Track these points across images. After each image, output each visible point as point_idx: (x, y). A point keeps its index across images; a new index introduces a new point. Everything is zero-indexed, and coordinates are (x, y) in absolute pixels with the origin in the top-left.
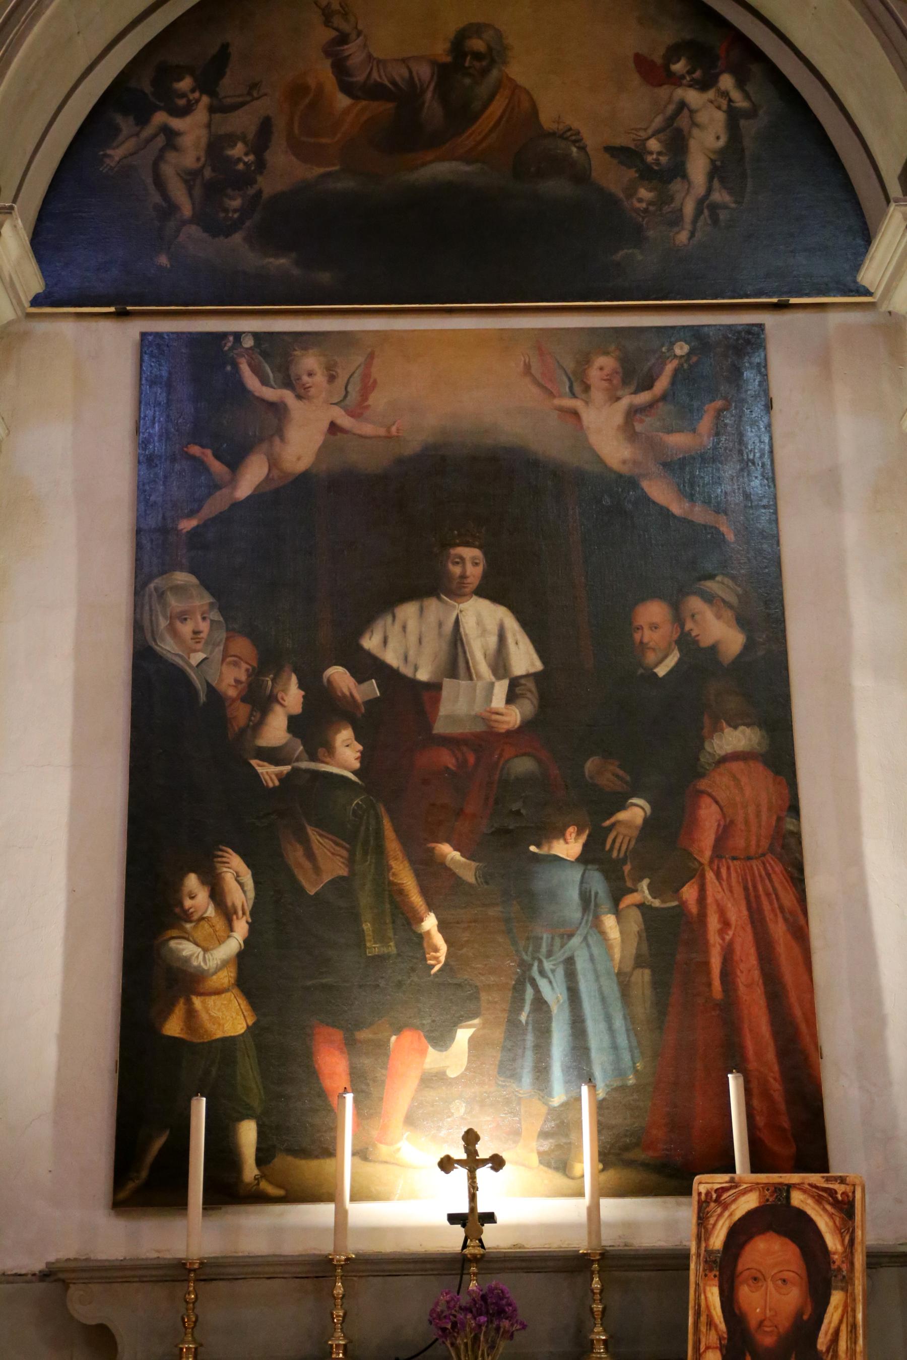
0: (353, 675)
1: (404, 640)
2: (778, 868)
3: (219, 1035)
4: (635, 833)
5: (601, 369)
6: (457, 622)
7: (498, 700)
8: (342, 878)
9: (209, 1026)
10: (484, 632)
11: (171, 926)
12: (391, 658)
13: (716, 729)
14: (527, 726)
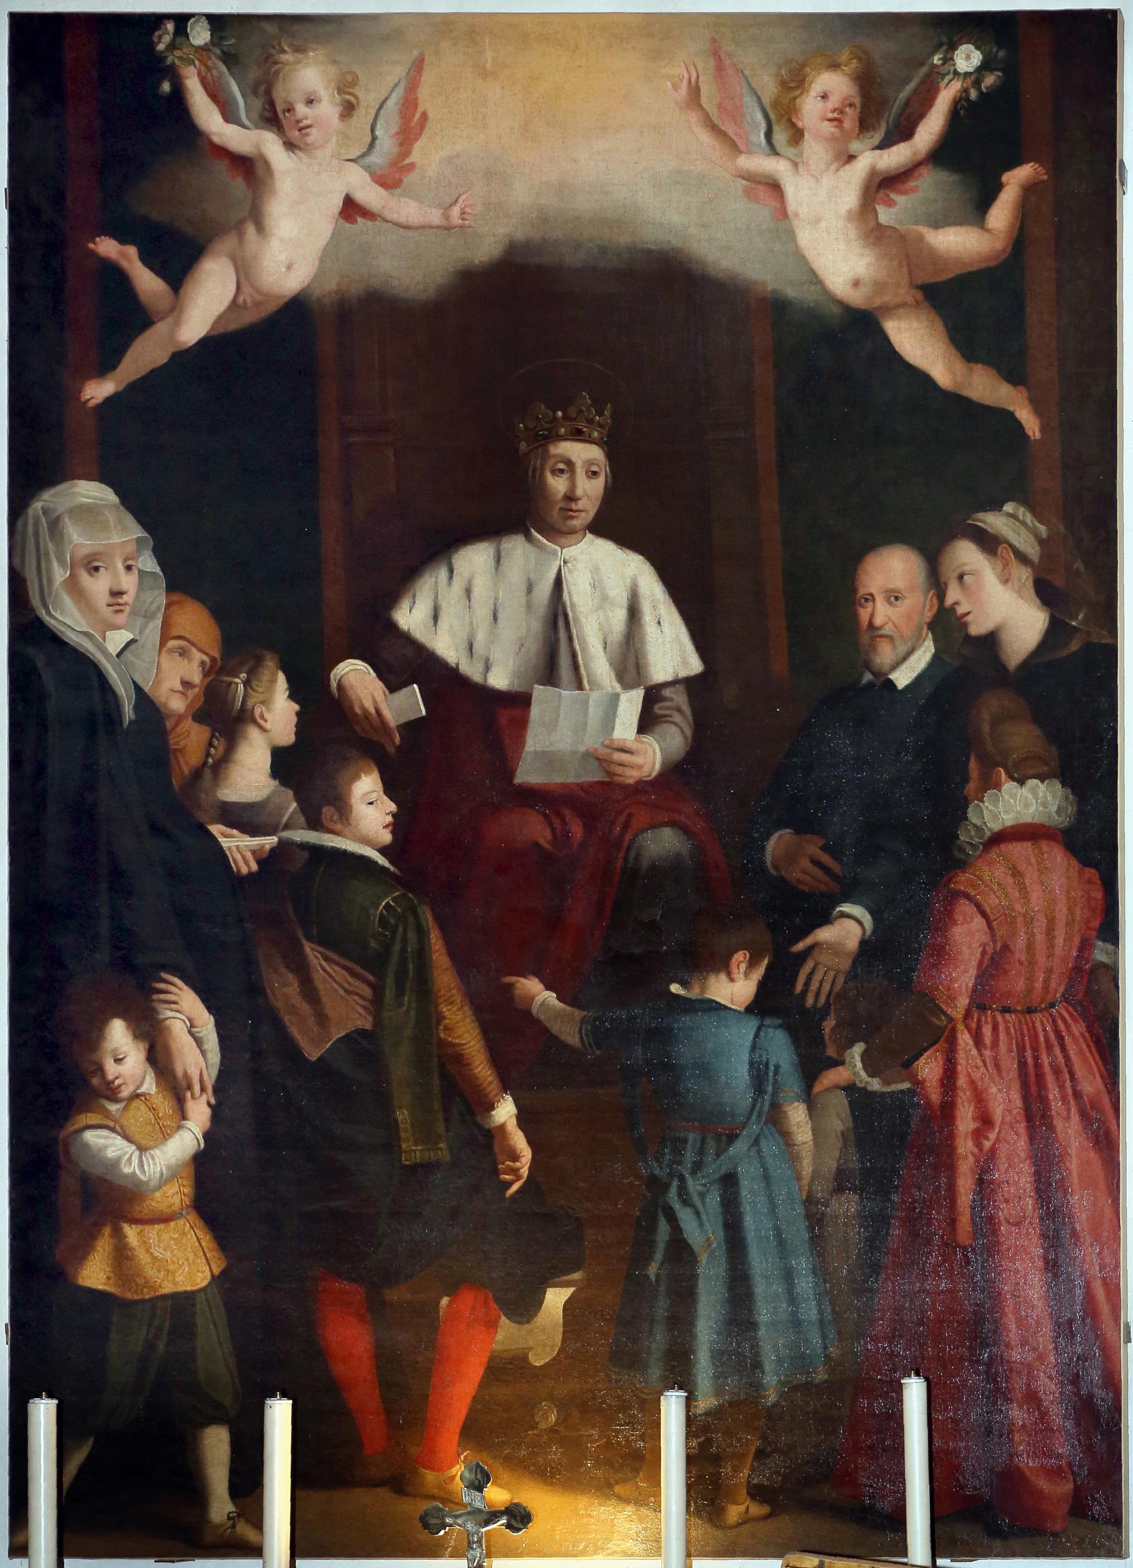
0: (381, 676)
1: (465, 610)
2: (1079, 1028)
3: (168, 1288)
4: (845, 964)
5: (824, 97)
6: (558, 583)
7: (625, 727)
8: (362, 1033)
9: (150, 1272)
10: (604, 600)
11: (85, 1108)
12: (446, 646)
13: (989, 783)
14: (676, 773)
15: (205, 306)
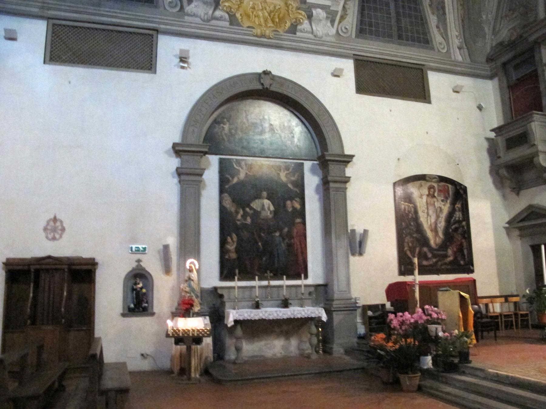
1: (256, 205)
7: (269, 214)
15: (235, 180)
